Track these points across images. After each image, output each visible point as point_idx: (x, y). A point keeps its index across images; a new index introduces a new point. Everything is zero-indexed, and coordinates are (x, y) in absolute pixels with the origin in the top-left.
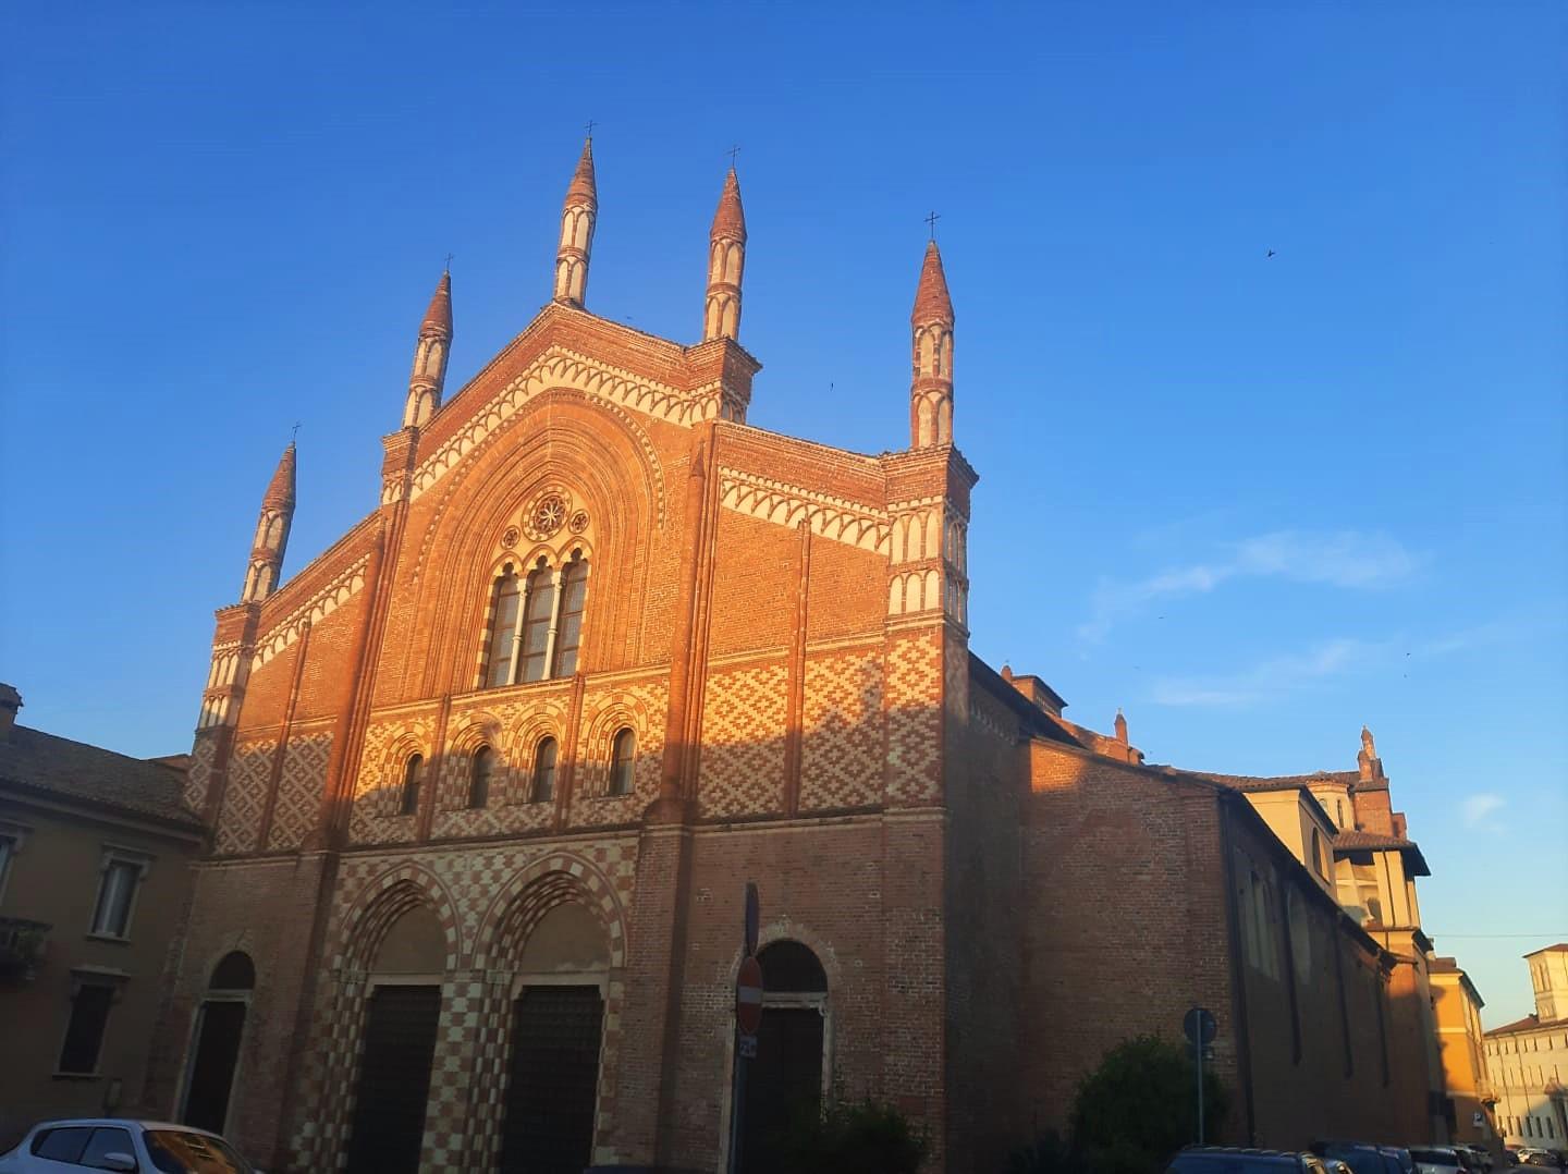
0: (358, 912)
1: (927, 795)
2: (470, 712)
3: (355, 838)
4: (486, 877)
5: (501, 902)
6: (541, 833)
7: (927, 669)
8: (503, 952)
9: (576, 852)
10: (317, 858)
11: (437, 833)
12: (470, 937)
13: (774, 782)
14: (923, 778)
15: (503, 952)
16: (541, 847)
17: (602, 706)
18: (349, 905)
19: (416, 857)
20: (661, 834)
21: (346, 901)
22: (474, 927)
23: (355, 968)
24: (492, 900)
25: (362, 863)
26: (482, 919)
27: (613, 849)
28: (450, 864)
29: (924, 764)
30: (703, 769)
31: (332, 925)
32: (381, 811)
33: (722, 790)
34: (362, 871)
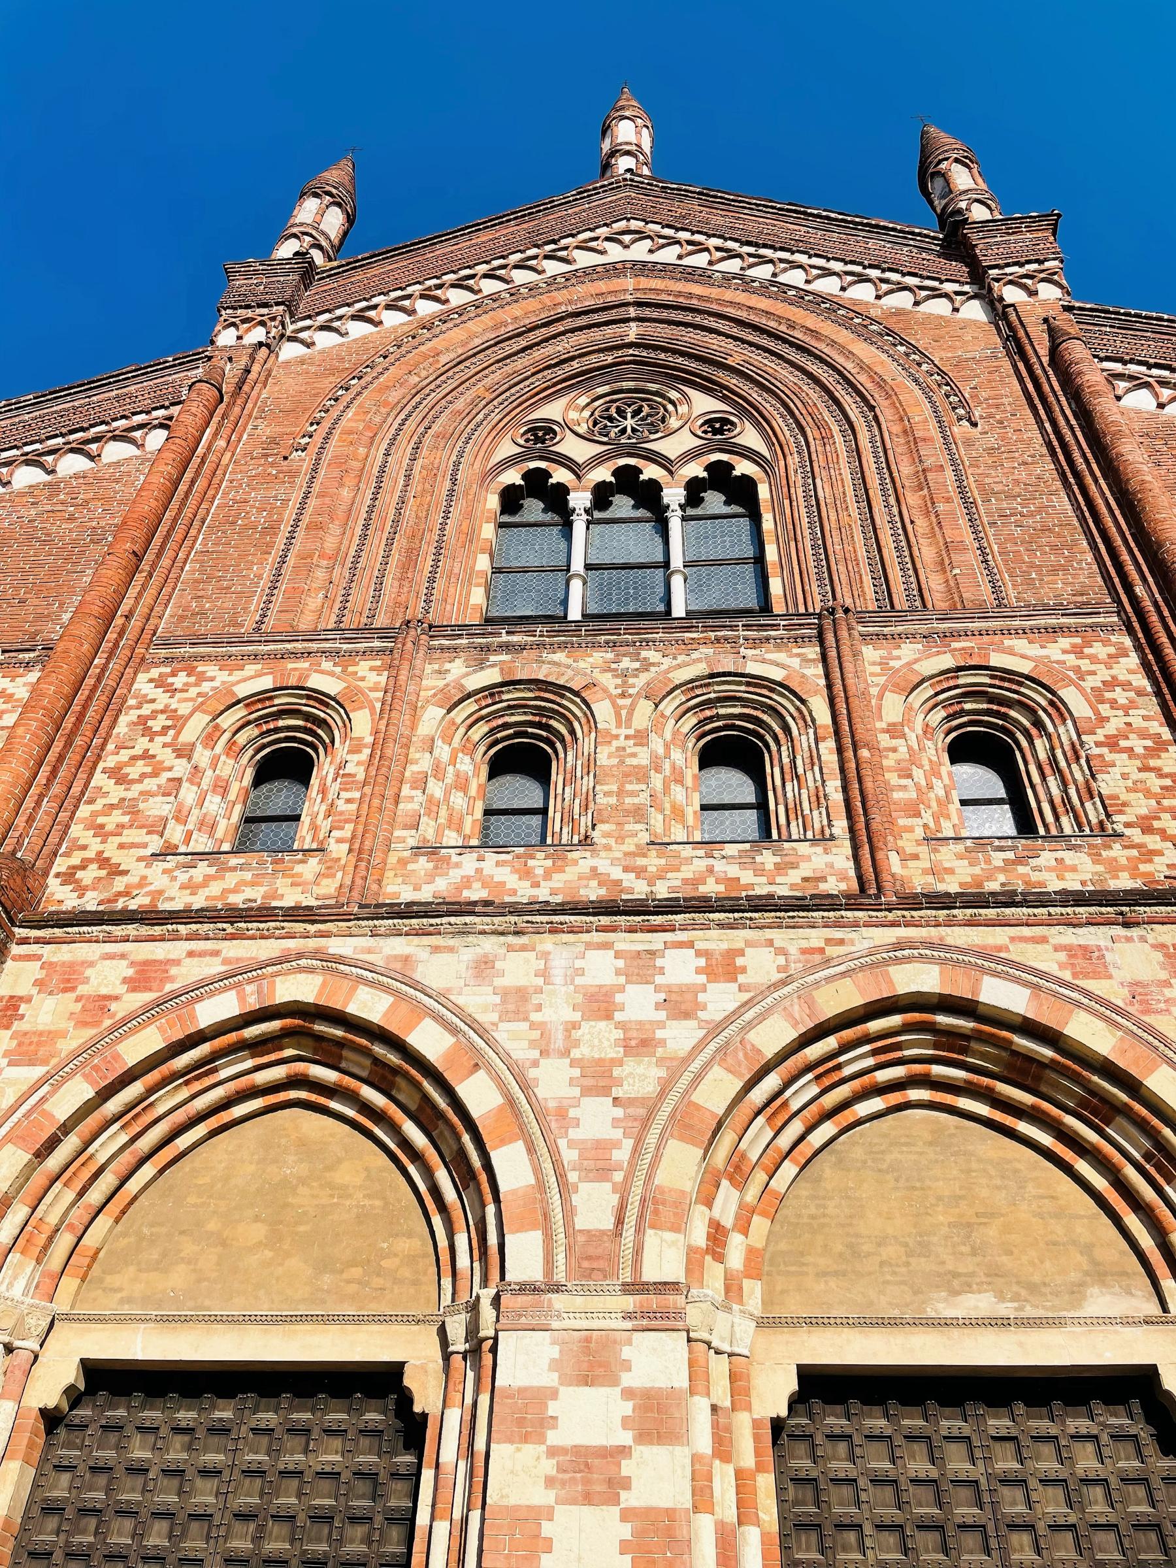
2: (493, 658)
5: (717, 1071)
11: (401, 891)
12: (602, 1172)
19: (337, 946)
22: (616, 1144)
25: (105, 965)
26: (646, 1123)
28: (484, 967)
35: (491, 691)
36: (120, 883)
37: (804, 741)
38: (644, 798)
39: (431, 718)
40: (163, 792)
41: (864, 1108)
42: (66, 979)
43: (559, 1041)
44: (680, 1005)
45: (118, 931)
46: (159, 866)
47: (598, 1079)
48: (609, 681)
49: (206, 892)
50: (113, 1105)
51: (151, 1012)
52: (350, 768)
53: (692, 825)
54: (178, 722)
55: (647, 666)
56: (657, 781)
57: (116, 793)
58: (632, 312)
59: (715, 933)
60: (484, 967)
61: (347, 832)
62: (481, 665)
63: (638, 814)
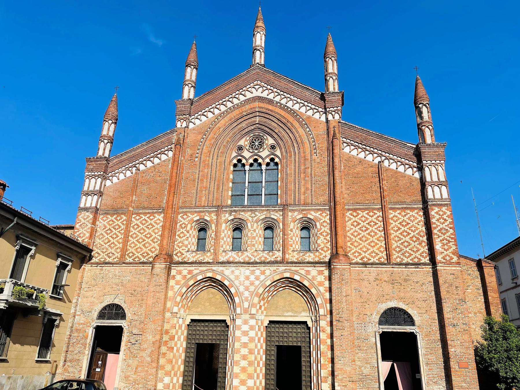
0: (184, 289)
1: (453, 261)
2: (233, 213)
3: (176, 258)
4: (252, 278)
5: (261, 288)
6: (276, 262)
7: (447, 218)
8: (261, 307)
9: (296, 271)
10: (164, 266)
11: (221, 259)
13: (381, 251)
14: (451, 255)
15: (261, 307)
16: (278, 268)
17: (298, 217)
18: (179, 286)
20: (341, 267)
23: (182, 311)
24: (256, 287)
25: (184, 270)
27: (314, 271)
28: (233, 272)
29: (450, 250)
30: (349, 244)
31: (170, 294)
32: (189, 249)
33: (358, 253)
34: (185, 272)
35: (233, 220)
36: (183, 256)
37: (279, 231)
38: (255, 242)
39: (224, 225)
40: (186, 242)
41: (280, 289)
42: (179, 272)
43: (242, 283)
44: (257, 278)
45: (185, 265)
46: (188, 253)
47: (247, 289)
48: (250, 219)
49: (195, 258)
50: (189, 290)
51: (191, 278)
52: (212, 236)
53: (261, 247)
54: (186, 227)
55: (256, 215)
56: (257, 238)
57: (180, 240)
58: (258, 114)
60: (233, 272)
61: (213, 248)
62: (230, 215)
63: (254, 245)
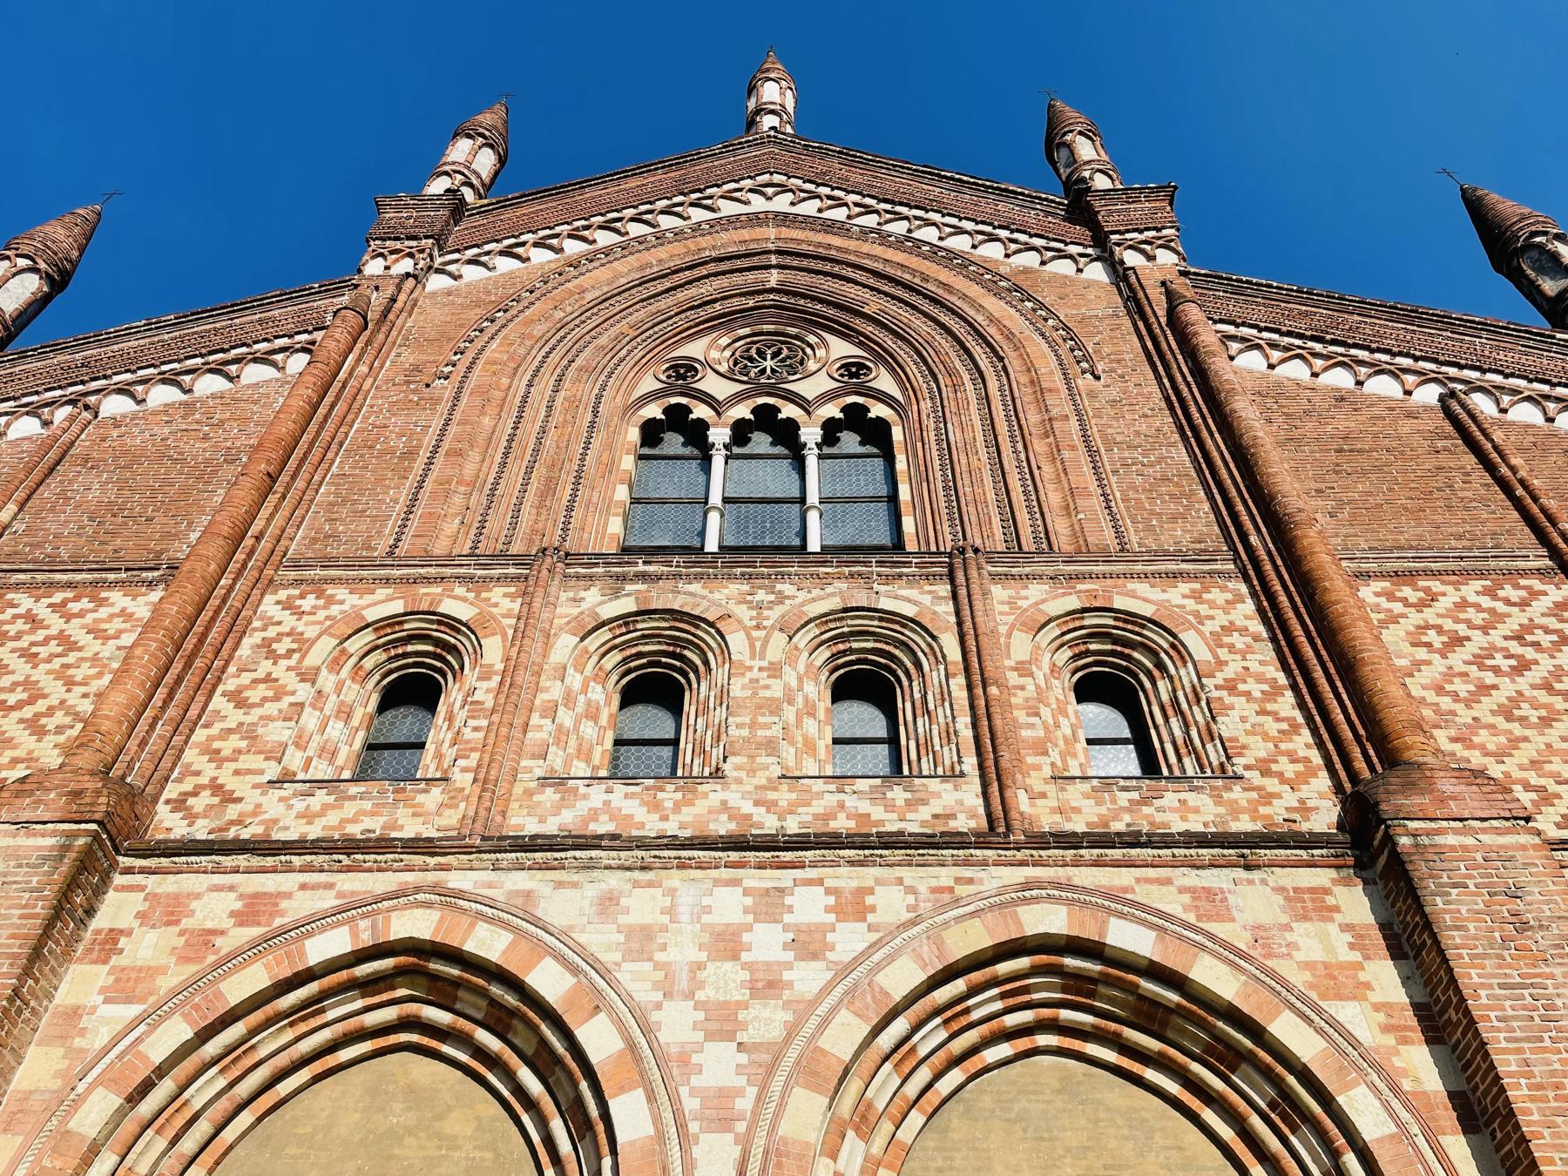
2: (629, 587)
4: (767, 943)
5: (844, 1015)
11: (525, 823)
12: (724, 1122)
21: (119, 992)
22: (739, 1092)
25: (211, 897)
26: (771, 1069)
28: (608, 904)
35: (626, 619)
36: (233, 811)
37: (935, 677)
38: (776, 731)
39: (565, 645)
40: (283, 719)
41: (992, 1054)
42: (171, 912)
43: (683, 983)
44: (808, 945)
45: (227, 861)
46: (276, 794)
47: (722, 1023)
48: (744, 613)
49: (323, 821)
50: (212, 1048)
51: (257, 948)
52: (479, 696)
53: (822, 759)
54: (303, 645)
55: (781, 598)
56: (790, 713)
57: (234, 716)
58: (774, 260)
59: (845, 870)
60: (608, 904)
61: (472, 760)
62: (616, 594)
63: (770, 747)
